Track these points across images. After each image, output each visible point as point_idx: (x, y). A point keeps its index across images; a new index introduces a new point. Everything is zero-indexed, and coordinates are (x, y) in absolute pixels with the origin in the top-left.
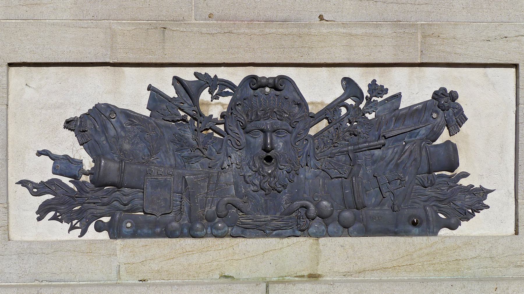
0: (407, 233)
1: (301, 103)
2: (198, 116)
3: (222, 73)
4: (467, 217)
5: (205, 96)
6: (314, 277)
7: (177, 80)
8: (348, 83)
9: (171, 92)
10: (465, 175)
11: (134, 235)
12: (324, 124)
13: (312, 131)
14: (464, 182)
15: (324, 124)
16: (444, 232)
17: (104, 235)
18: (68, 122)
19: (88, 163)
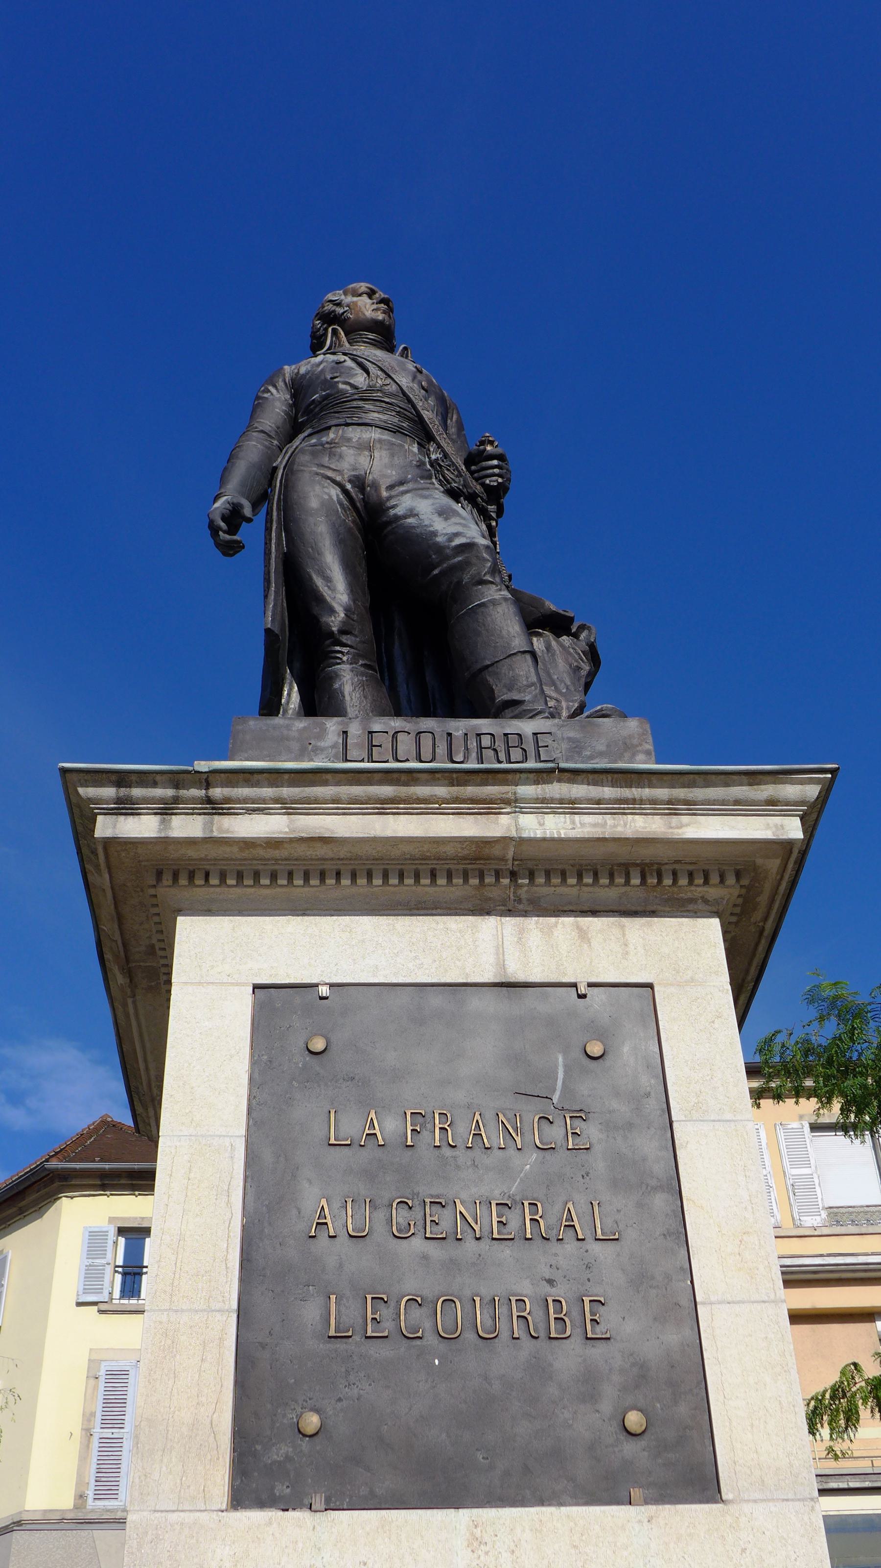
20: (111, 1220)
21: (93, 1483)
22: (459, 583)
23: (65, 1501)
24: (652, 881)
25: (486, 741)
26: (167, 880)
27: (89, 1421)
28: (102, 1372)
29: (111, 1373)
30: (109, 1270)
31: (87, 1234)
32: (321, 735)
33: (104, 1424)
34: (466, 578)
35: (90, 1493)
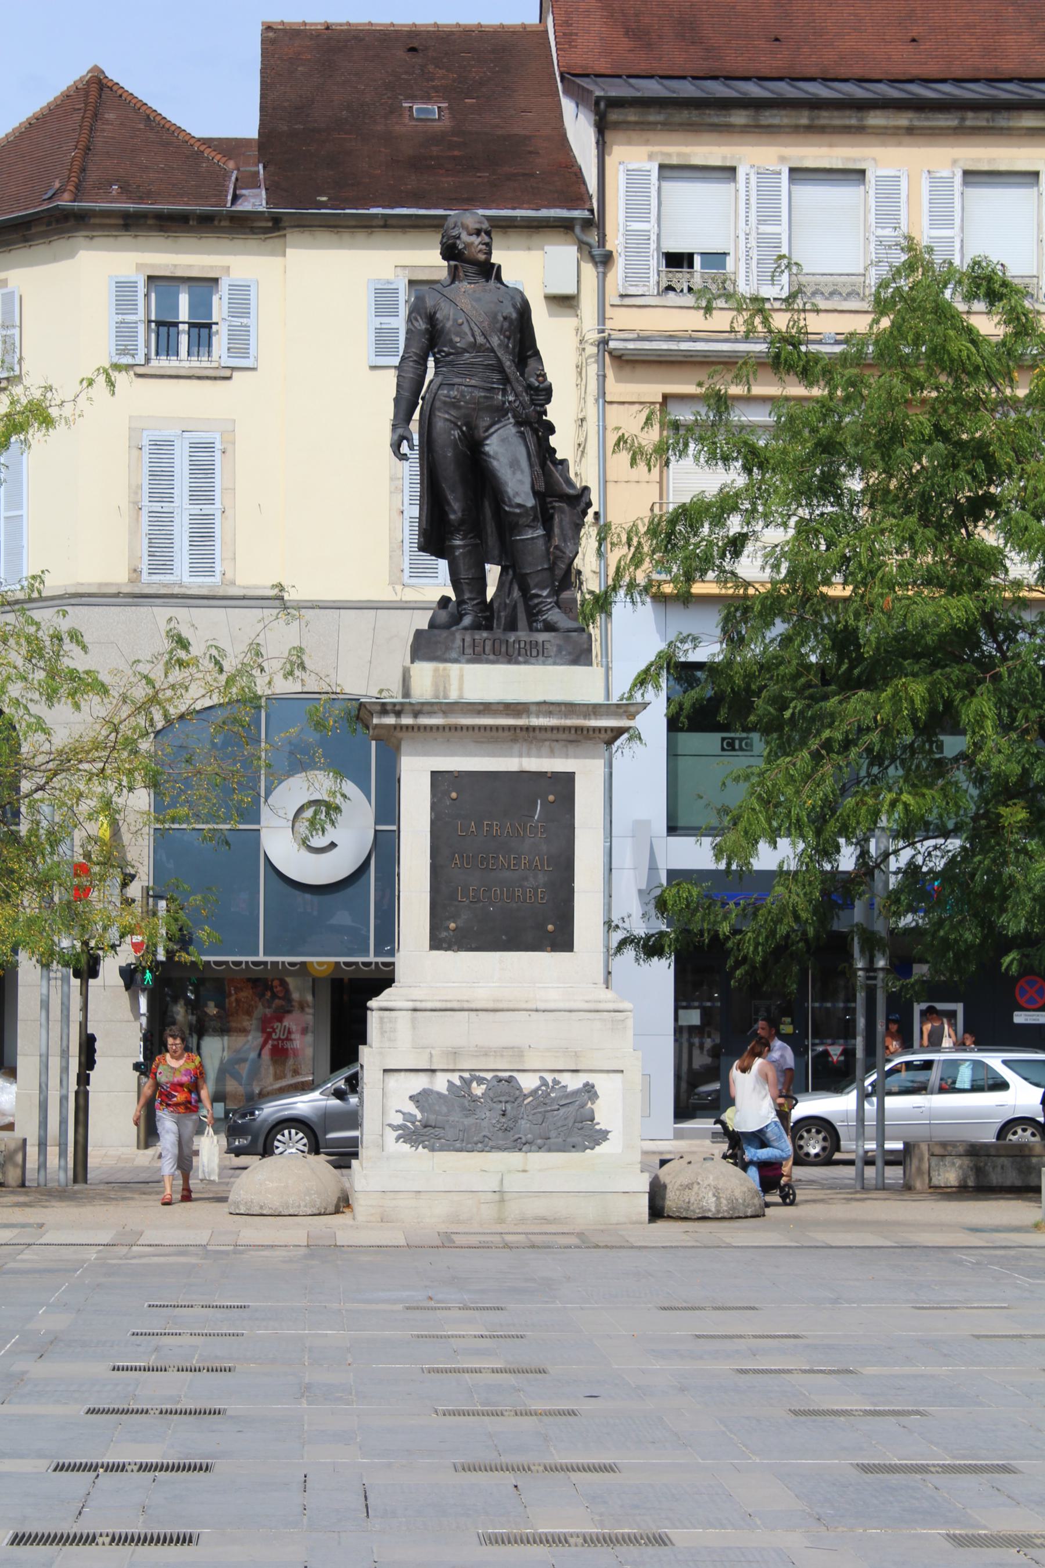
0: (569, 1151)
1: (520, 1089)
2: (470, 1094)
3: (482, 1074)
4: (599, 1144)
5: (474, 1084)
6: (524, 1171)
7: (461, 1077)
8: (542, 1078)
9: (458, 1083)
10: (598, 1124)
11: (440, 1150)
12: (531, 1099)
13: (526, 1102)
14: (597, 1127)
15: (531, 1099)
16: (588, 1151)
17: (426, 1150)
18: (411, 1097)
19: (419, 1116)
20: (139, 267)
21: (146, 558)
22: (517, 524)
23: (118, 576)
24: (579, 732)
25: (522, 645)
26: (398, 729)
27: (136, 493)
28: (145, 442)
29: (155, 444)
30: (141, 328)
31: (114, 285)
32: (453, 641)
33: (153, 497)
34: (520, 522)
35: (145, 568)
